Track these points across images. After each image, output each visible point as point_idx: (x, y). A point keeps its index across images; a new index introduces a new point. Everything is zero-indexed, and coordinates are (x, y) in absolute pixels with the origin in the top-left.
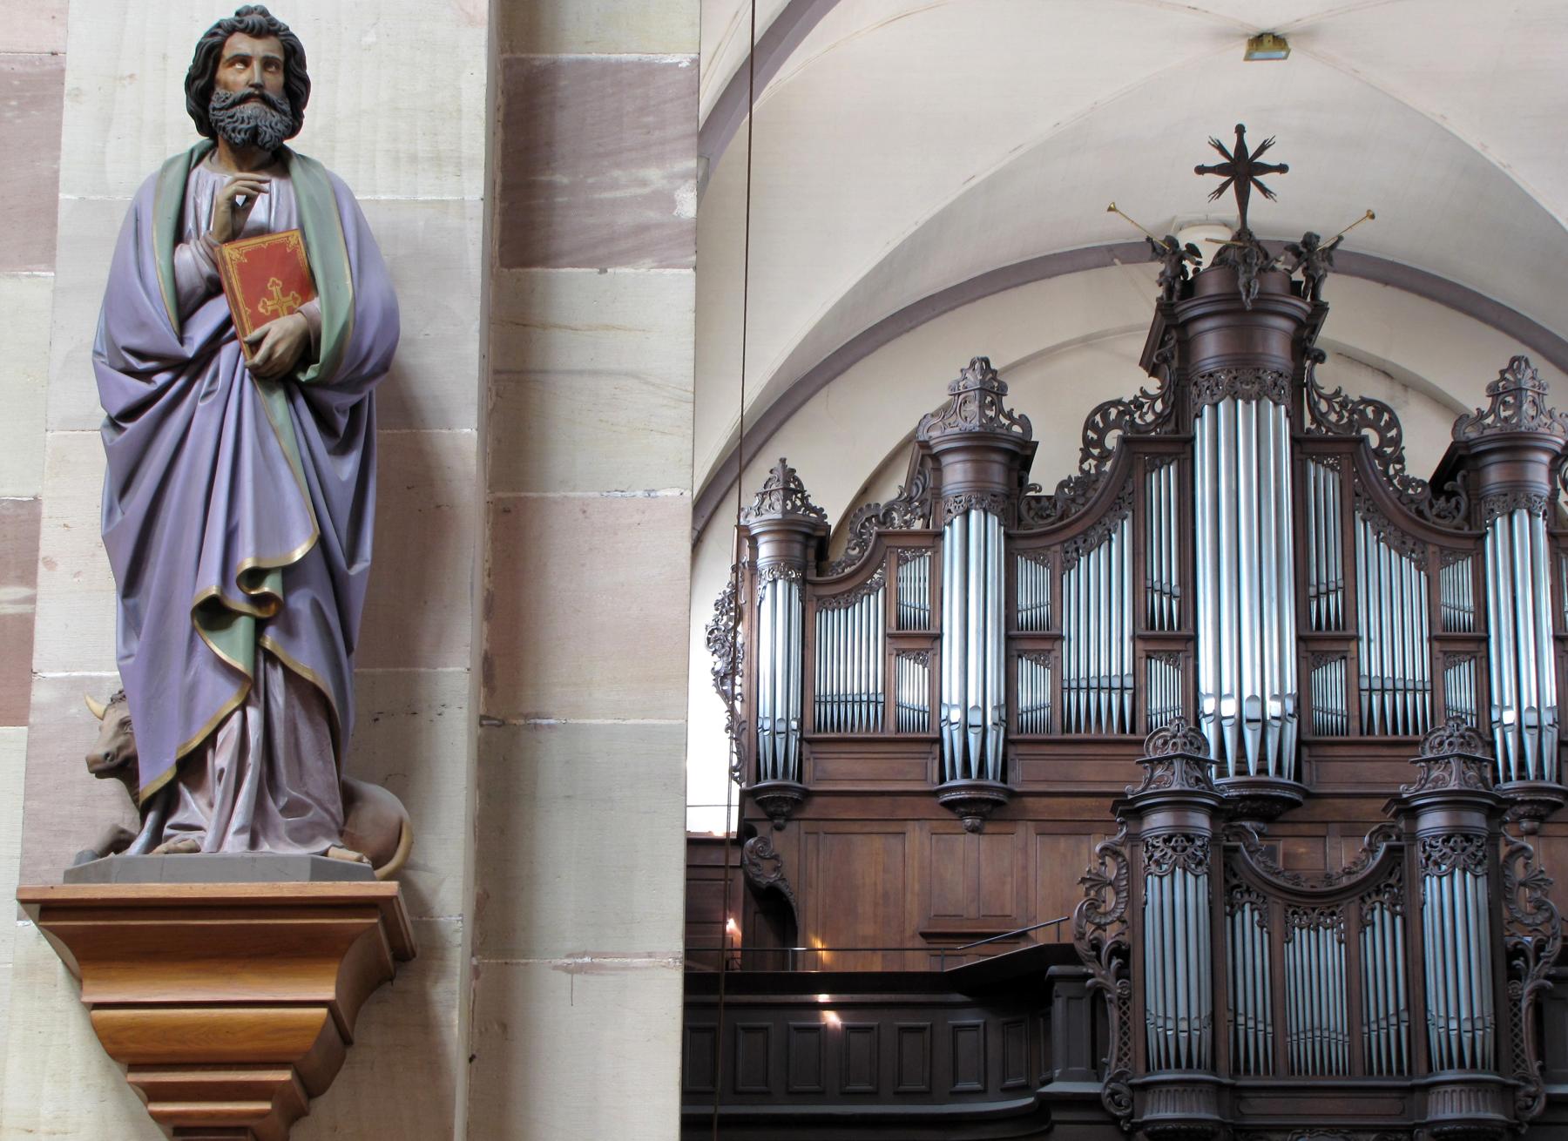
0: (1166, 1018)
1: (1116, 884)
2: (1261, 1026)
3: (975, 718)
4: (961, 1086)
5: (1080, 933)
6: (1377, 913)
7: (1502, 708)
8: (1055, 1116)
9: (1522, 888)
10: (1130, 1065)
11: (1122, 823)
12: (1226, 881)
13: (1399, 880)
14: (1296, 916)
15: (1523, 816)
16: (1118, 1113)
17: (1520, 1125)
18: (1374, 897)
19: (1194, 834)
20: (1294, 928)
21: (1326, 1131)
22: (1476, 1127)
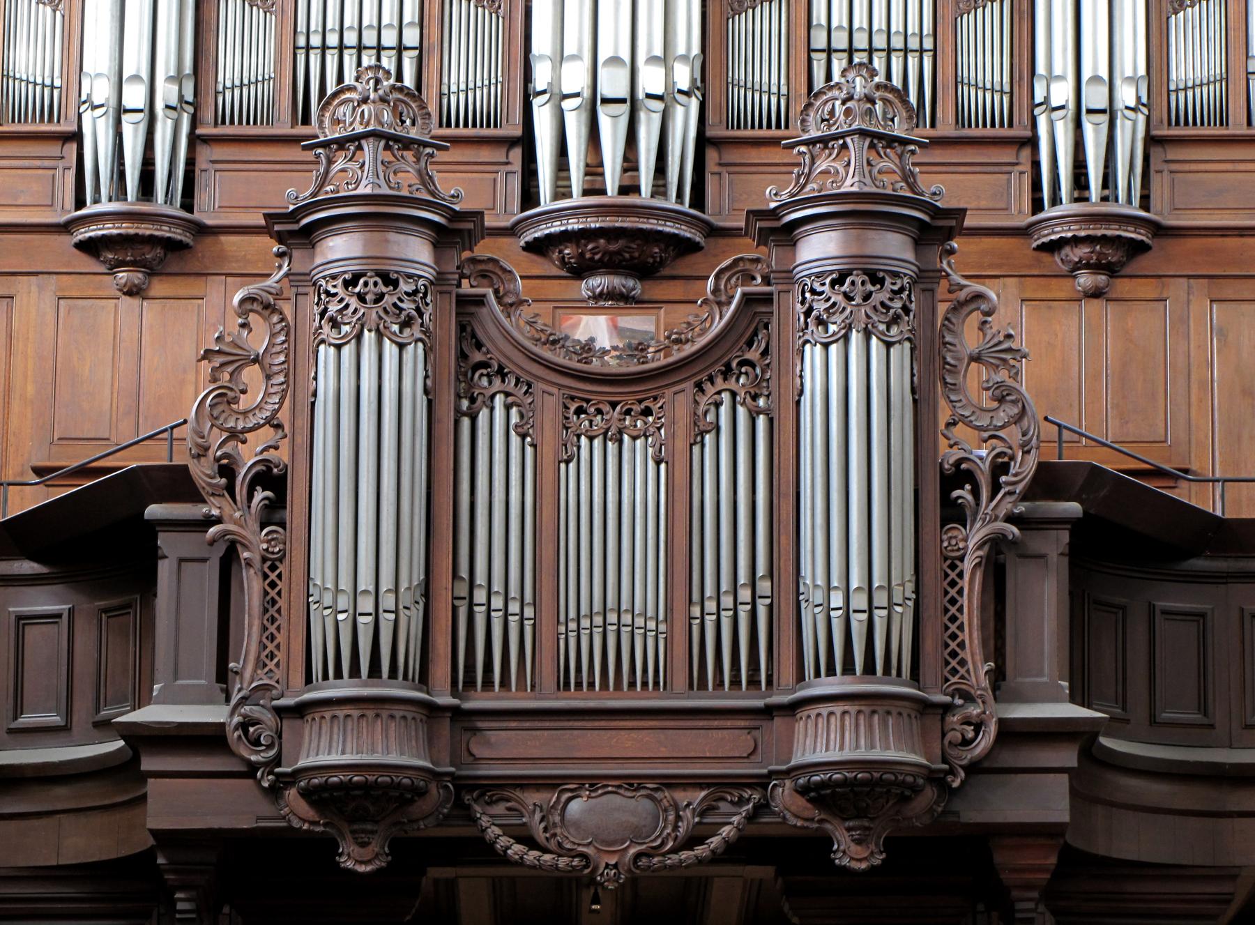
0: (337, 590)
1: (268, 360)
2: (514, 607)
3: (135, 96)
4: (26, 720)
5: (198, 445)
6: (724, 410)
7: (1050, 78)
8: (147, 764)
9: (973, 364)
10: (278, 674)
11: (281, 255)
12: (463, 356)
13: (765, 353)
14: (583, 416)
15: (1077, 266)
16: (253, 758)
17: (952, 771)
18: (720, 383)
19: (397, 272)
20: (579, 437)
21: (619, 787)
22: (867, 775)
